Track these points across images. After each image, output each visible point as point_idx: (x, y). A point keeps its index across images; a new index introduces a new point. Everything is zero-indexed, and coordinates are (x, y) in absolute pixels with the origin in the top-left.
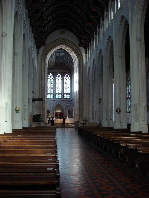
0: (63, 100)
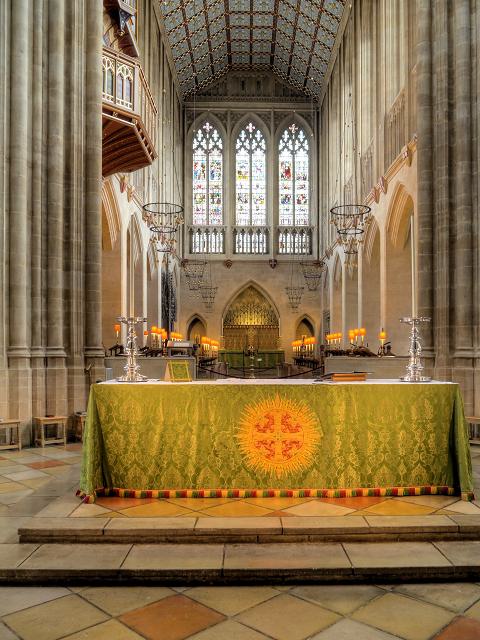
0: (274, 264)
